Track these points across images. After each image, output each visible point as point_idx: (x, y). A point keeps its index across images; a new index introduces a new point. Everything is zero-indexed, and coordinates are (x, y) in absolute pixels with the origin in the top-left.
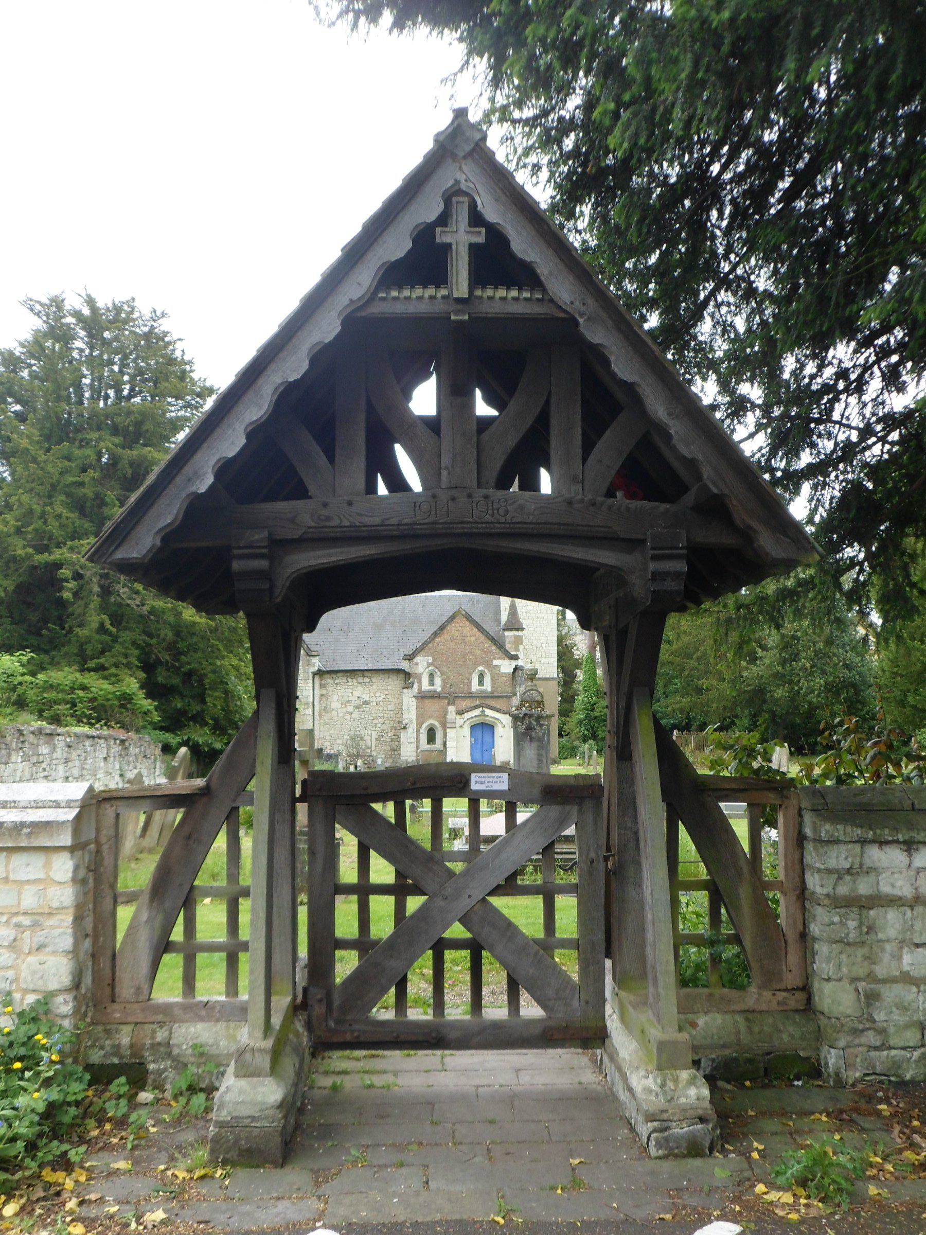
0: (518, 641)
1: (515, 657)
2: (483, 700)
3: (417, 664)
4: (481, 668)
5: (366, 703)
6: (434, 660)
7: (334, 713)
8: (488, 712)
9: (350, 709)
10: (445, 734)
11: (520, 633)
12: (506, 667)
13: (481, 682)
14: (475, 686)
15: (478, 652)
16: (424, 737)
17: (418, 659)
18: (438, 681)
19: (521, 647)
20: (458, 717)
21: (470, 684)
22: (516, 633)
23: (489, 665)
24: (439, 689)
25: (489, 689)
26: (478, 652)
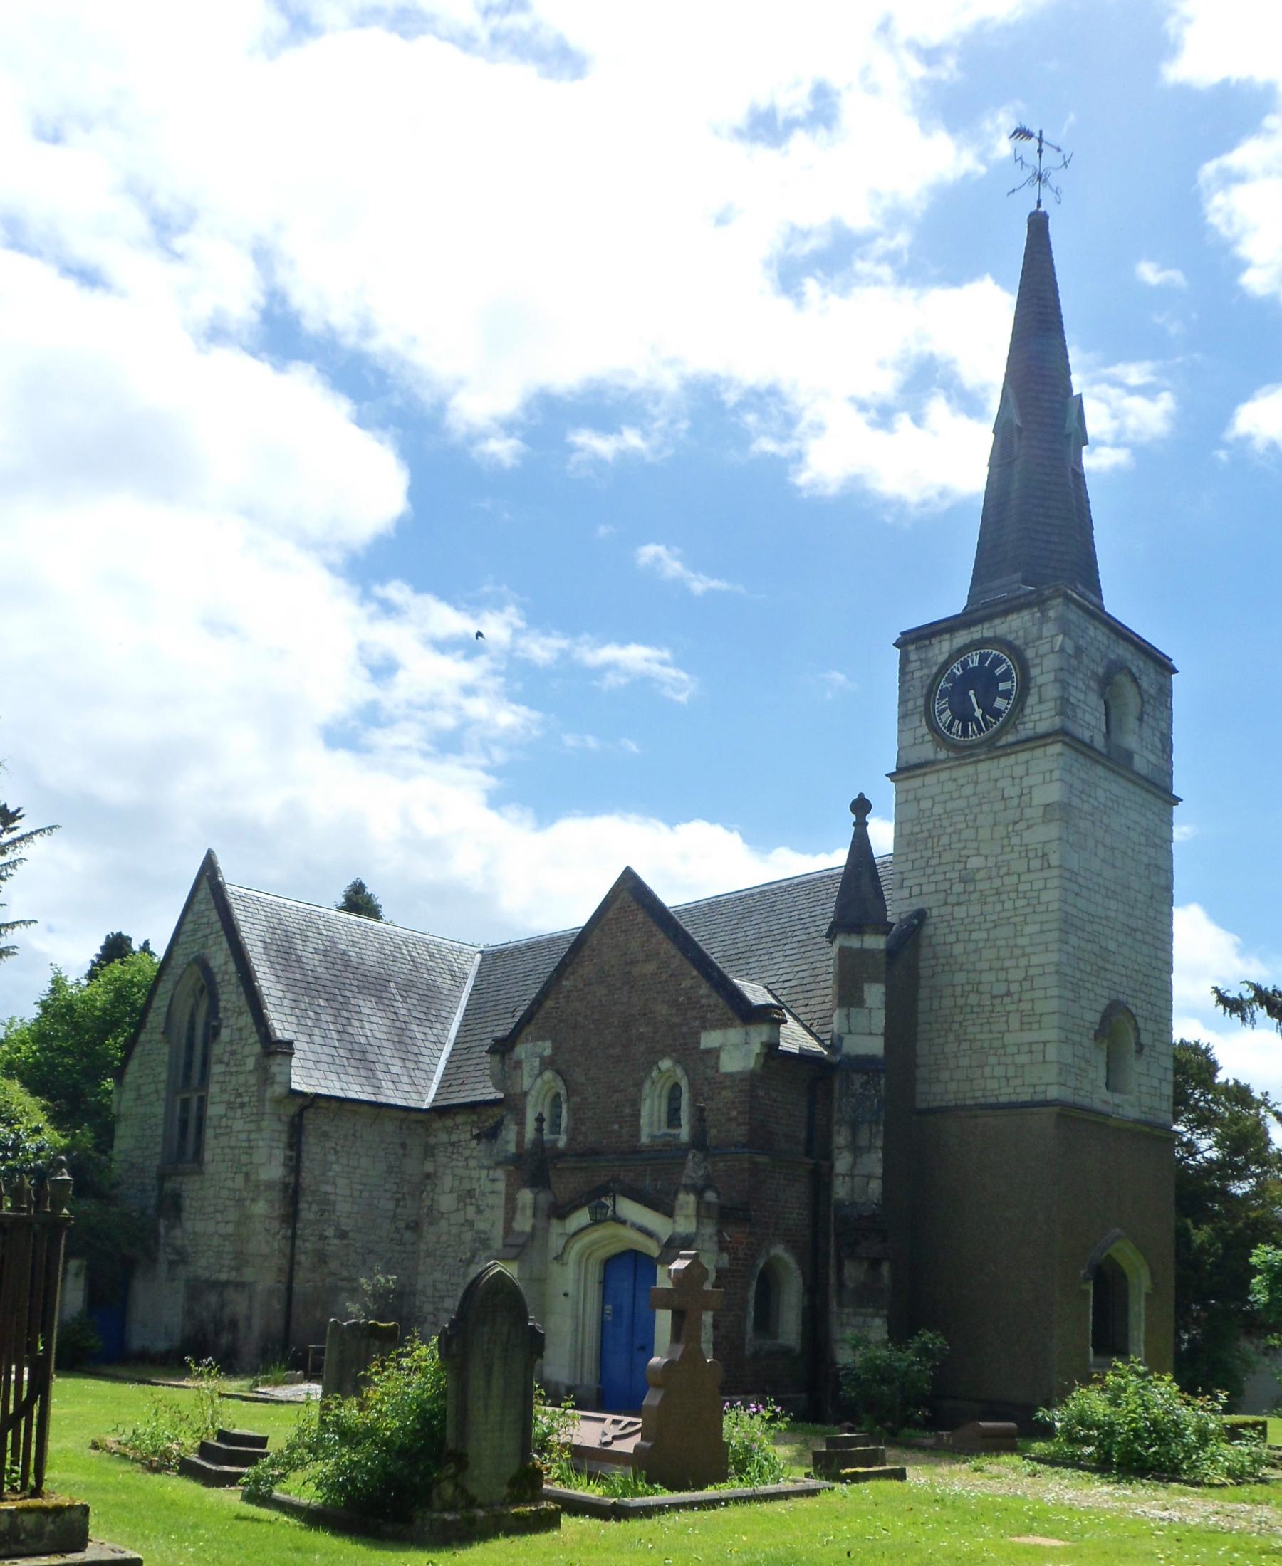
6: (556, 1048)
13: (673, 1117)
14: (651, 1120)
15: (662, 1010)
21: (637, 1116)
22: (854, 942)
26: (662, 1010)
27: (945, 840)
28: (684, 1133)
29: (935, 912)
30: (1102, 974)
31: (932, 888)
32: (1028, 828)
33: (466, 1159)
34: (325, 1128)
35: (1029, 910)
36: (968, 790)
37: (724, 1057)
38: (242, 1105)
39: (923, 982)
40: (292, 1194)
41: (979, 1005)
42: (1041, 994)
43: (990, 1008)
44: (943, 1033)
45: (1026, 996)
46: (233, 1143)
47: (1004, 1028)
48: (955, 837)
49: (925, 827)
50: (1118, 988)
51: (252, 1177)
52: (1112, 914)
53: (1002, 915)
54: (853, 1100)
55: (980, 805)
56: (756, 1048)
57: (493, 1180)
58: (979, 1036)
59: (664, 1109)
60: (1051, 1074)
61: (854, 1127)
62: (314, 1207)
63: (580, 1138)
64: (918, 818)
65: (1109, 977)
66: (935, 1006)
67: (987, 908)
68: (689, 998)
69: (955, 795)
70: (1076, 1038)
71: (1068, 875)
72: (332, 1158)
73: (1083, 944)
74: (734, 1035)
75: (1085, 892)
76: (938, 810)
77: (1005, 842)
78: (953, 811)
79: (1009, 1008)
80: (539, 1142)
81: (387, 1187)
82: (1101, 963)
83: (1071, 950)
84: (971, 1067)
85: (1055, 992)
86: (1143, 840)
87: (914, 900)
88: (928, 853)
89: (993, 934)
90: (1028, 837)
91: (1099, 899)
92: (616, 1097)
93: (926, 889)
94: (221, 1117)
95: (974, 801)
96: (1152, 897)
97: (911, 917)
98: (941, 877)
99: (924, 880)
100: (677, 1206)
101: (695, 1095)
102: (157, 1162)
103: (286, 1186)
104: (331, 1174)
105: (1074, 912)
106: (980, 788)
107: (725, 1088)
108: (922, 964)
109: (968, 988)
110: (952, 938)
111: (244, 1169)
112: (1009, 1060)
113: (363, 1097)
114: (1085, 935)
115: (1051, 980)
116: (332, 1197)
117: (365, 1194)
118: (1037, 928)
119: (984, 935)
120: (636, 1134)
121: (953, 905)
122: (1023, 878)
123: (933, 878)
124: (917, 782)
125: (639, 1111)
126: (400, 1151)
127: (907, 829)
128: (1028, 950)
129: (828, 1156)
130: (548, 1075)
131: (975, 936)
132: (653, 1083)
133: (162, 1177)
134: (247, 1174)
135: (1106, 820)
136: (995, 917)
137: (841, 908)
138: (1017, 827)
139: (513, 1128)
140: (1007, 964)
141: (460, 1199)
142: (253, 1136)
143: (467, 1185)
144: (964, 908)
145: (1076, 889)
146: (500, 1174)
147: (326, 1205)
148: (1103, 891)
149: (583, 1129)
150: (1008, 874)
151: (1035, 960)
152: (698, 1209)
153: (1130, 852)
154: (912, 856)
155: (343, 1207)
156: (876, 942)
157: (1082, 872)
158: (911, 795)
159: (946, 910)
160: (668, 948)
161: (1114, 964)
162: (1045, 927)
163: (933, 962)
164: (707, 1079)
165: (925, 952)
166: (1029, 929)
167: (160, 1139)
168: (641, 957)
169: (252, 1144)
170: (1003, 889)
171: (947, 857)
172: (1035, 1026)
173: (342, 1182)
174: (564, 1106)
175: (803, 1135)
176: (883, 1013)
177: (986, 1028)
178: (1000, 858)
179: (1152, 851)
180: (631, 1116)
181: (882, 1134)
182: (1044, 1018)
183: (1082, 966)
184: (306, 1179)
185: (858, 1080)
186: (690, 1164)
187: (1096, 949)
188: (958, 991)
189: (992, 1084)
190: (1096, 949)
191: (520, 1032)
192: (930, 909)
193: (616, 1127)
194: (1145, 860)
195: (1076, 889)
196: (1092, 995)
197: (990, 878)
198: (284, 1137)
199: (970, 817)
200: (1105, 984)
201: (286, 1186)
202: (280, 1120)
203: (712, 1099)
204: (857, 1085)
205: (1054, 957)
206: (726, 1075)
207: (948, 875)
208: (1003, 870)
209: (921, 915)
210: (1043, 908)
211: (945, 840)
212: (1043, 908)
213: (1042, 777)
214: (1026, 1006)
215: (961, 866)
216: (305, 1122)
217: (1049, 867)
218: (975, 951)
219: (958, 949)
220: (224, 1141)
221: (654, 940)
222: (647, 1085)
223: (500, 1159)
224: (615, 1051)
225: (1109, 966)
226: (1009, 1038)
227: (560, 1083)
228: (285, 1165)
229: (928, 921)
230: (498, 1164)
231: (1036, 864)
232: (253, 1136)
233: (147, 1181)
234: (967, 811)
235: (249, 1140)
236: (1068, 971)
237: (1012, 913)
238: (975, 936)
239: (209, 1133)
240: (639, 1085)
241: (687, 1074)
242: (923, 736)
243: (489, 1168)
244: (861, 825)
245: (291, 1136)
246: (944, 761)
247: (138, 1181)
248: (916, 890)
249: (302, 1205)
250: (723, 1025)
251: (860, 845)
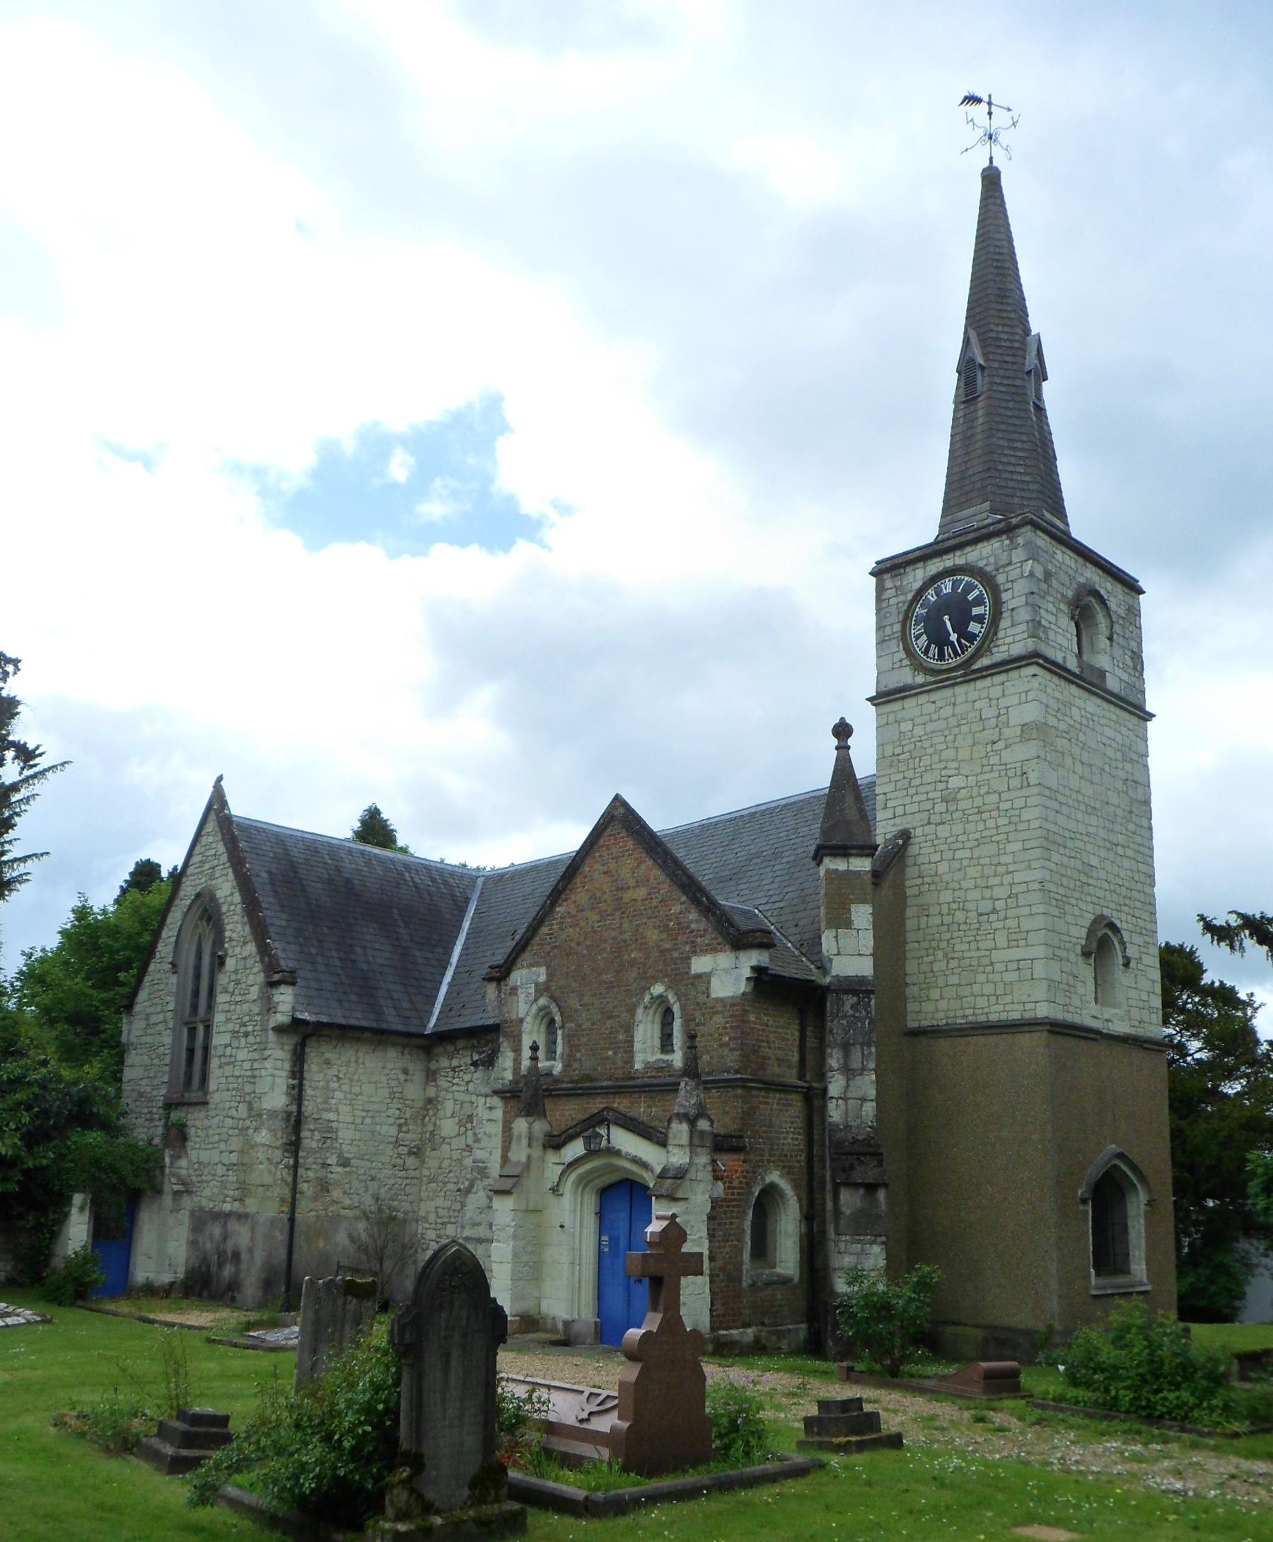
3: (514, 990)
4: (658, 989)
6: (550, 976)
7: (446, 1148)
12: (727, 975)
13: (666, 1043)
14: (645, 1047)
15: (653, 935)
17: (518, 976)
20: (552, 1157)
21: (630, 1042)
22: (840, 865)
26: (653, 935)
27: (926, 761)
28: (677, 1059)
29: (919, 832)
30: (1086, 889)
31: (915, 808)
32: (1006, 747)
33: (468, 1083)
34: (328, 1055)
35: (1012, 828)
36: (947, 711)
37: (715, 982)
38: (246, 1035)
39: (909, 901)
40: (295, 1122)
41: (965, 923)
42: (1026, 911)
43: (977, 926)
44: (931, 951)
45: (1011, 913)
46: (237, 1073)
47: (991, 944)
48: (936, 758)
49: (906, 749)
50: (1102, 902)
51: (255, 1105)
52: (1092, 830)
53: (985, 833)
54: (844, 1022)
55: (959, 726)
56: (747, 973)
57: (491, 1108)
58: (966, 955)
59: (657, 1034)
60: (1040, 992)
61: (846, 1048)
62: (317, 1135)
63: (576, 1065)
64: (899, 740)
65: (1092, 892)
66: (923, 926)
67: (970, 827)
68: (679, 924)
69: (935, 717)
70: (1063, 954)
71: (1047, 793)
72: (334, 1085)
73: (1065, 860)
74: (724, 959)
75: (1065, 810)
76: (919, 731)
77: (985, 761)
78: (933, 732)
79: (995, 925)
80: (534, 1069)
81: (390, 1112)
82: (1084, 879)
83: (1053, 867)
84: (959, 985)
85: (1041, 909)
86: (1119, 755)
87: (897, 820)
88: (909, 774)
89: (977, 853)
90: (1007, 756)
91: (1080, 816)
92: (609, 1023)
93: (909, 809)
94: (226, 1046)
95: (953, 722)
96: (1131, 812)
97: (896, 837)
98: (924, 797)
99: (908, 800)
100: (670, 1135)
101: (687, 1020)
102: (163, 1092)
103: (289, 1114)
104: (333, 1101)
105: (1055, 829)
106: (958, 710)
107: (717, 1013)
108: (908, 883)
109: (955, 906)
110: (936, 857)
111: (247, 1098)
112: (997, 977)
113: (364, 1023)
114: (1067, 852)
115: (1035, 897)
116: (334, 1125)
117: (368, 1121)
118: (1018, 846)
119: (968, 854)
120: (630, 1061)
121: (937, 825)
122: (1004, 796)
123: (916, 798)
124: (897, 706)
125: (632, 1036)
126: (402, 1077)
127: (888, 752)
128: (1011, 868)
129: (822, 1075)
130: (542, 1001)
131: (959, 854)
132: (646, 1008)
133: (169, 1106)
134: (250, 1103)
135: (1082, 737)
136: (977, 835)
137: (825, 832)
138: (996, 747)
139: (511, 1055)
140: (992, 881)
141: (460, 1124)
142: (256, 1065)
143: (467, 1110)
144: (947, 827)
145: (1057, 806)
146: (496, 1101)
147: (329, 1132)
148: (1083, 807)
149: (578, 1055)
150: (988, 793)
151: (1018, 877)
152: (691, 1138)
153: (1107, 768)
154: (894, 778)
155: (346, 1134)
156: (862, 865)
157: (1061, 789)
158: (891, 719)
159: (929, 829)
161: (1098, 879)
162: (1028, 845)
163: (919, 881)
164: (698, 1004)
165: (911, 871)
166: (1011, 847)
167: (167, 1069)
168: (632, 883)
169: (256, 1073)
170: (986, 807)
171: (928, 777)
172: (1022, 943)
173: (342, 1108)
174: (559, 1032)
175: (795, 1058)
176: (871, 933)
177: (973, 945)
178: (980, 778)
179: (1128, 766)
180: (626, 1042)
181: (874, 1056)
182: (1031, 935)
183: (1065, 882)
184: (309, 1107)
185: (850, 1000)
186: (682, 1093)
187: (1079, 865)
188: (945, 911)
189: (981, 1002)
190: (1079, 865)
191: (515, 960)
192: (914, 828)
193: (610, 1053)
194: (1123, 775)
195: (1057, 806)
196: (1077, 912)
197: (971, 797)
198: (287, 1066)
199: (950, 738)
200: (1089, 899)
201: (289, 1114)
202: (282, 1049)
203: (703, 1025)
204: (847, 1007)
205: (1038, 874)
206: (717, 1000)
207: (930, 796)
208: (984, 790)
209: (906, 835)
210: (1025, 826)
211: (926, 761)
212: (1025, 826)
213: (1025, 698)
214: (1011, 923)
215: (943, 786)
216: (307, 1050)
217: (1029, 785)
218: (960, 870)
219: (943, 867)
220: (228, 1070)
221: (643, 867)
222: (640, 1011)
223: (498, 1086)
224: (608, 977)
225: (1090, 881)
226: (996, 956)
227: (554, 1009)
228: (288, 1094)
229: (912, 841)
230: (496, 1092)
231: (1015, 782)
232: (256, 1065)
233: (155, 1110)
234: (947, 732)
235: (252, 1069)
236: (1052, 887)
237: (994, 832)
238: (959, 854)
239: (214, 1063)
240: (632, 1011)
241: (679, 999)
242: (901, 661)
243: (486, 1096)
244: (843, 749)
245: (294, 1065)
246: (922, 685)
247: (145, 1111)
248: (900, 811)
249: (304, 1134)
250: (713, 950)
251: (843, 769)
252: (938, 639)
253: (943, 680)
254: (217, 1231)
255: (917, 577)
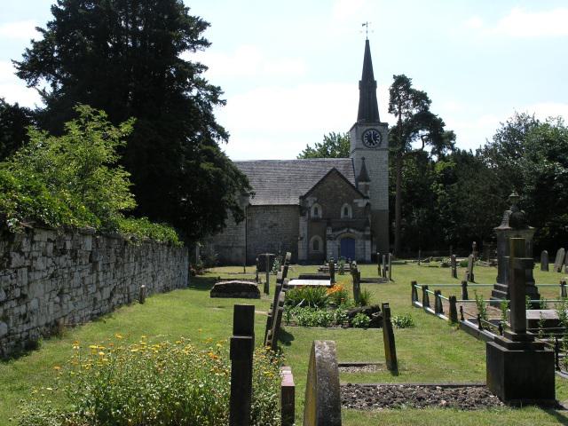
0: (367, 188)
1: (367, 198)
2: (348, 224)
5: (275, 225)
8: (352, 230)
9: (266, 228)
10: (325, 244)
11: (368, 183)
13: (346, 212)
16: (311, 245)
17: (308, 199)
18: (320, 212)
19: (369, 192)
23: (351, 203)
24: (321, 217)
25: (351, 217)
26: (344, 195)
74: (361, 200)
101: (353, 210)
160: (345, 183)
252: (371, 141)
253: (371, 149)
254: (227, 250)
255: (365, 128)
